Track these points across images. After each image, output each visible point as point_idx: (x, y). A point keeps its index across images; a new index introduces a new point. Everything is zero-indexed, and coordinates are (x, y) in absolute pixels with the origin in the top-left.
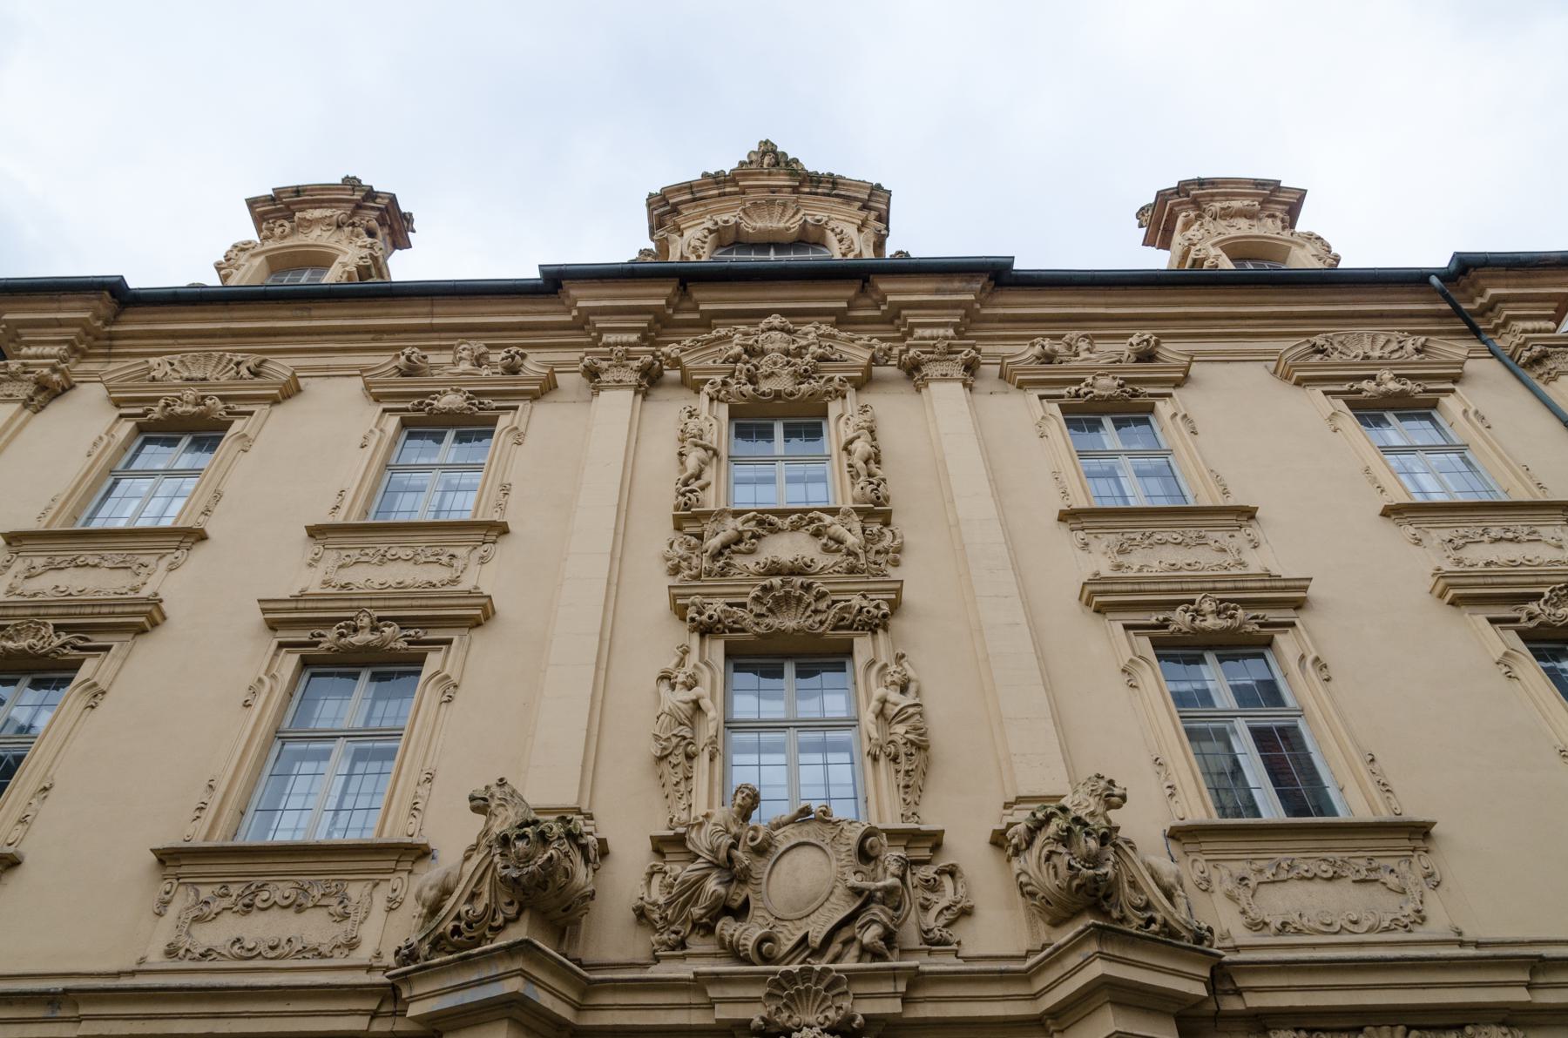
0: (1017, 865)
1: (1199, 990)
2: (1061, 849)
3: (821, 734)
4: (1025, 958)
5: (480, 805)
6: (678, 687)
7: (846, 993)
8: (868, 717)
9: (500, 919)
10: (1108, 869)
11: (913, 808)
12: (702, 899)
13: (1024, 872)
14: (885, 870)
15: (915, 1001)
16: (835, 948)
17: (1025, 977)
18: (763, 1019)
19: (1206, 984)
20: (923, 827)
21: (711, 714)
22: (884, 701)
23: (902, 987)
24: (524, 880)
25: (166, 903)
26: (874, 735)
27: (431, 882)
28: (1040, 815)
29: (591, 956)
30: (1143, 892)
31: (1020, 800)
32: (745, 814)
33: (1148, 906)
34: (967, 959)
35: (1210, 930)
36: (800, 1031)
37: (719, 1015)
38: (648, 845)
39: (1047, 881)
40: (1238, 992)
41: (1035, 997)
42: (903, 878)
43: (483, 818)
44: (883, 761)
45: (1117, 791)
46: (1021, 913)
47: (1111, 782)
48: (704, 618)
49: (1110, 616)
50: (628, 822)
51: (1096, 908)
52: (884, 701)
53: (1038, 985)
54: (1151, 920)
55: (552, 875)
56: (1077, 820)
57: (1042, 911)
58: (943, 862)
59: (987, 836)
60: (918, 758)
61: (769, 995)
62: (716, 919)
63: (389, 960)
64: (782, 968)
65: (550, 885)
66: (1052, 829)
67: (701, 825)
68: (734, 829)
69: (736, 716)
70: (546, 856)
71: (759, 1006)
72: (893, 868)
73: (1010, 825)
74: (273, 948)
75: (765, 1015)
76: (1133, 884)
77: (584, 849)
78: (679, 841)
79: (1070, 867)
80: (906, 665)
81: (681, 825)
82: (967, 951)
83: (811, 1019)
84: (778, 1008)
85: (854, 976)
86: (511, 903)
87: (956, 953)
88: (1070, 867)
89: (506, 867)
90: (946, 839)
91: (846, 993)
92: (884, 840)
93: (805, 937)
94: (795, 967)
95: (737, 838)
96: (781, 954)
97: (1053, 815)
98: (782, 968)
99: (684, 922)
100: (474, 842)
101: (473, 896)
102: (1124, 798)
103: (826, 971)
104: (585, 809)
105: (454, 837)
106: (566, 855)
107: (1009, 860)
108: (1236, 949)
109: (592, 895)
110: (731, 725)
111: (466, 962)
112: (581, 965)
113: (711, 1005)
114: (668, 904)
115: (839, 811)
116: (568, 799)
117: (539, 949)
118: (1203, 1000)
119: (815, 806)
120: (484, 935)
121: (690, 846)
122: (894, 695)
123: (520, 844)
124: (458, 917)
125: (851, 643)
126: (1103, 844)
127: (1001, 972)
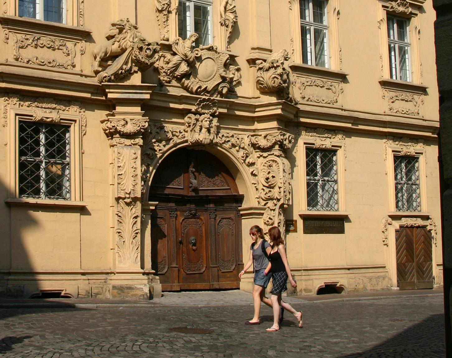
25: (8, 39)
74: (50, 63)
103: (214, 99)
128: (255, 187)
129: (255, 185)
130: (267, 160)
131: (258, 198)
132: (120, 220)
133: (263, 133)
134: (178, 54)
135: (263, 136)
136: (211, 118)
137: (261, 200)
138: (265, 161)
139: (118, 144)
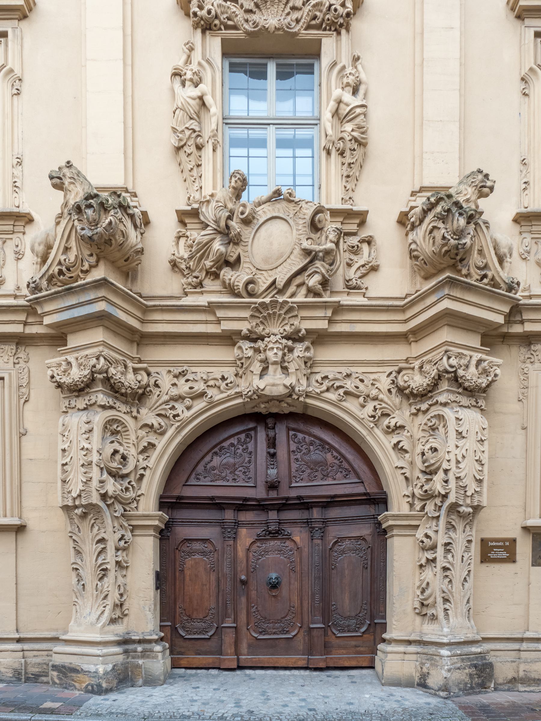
0: (411, 237)
1: (500, 319)
2: (441, 225)
3: (291, 132)
4: (405, 298)
5: (58, 182)
6: (188, 83)
7: (297, 316)
8: (327, 115)
9: (86, 267)
10: (467, 240)
11: (350, 194)
12: (211, 256)
13: (414, 242)
14: (327, 237)
15: (336, 322)
16: (292, 289)
17: (403, 309)
18: (248, 330)
19: (505, 316)
20: (355, 208)
21: (213, 110)
22: (339, 102)
23: (329, 313)
24: (95, 238)
26: (330, 132)
27: (38, 240)
28: (432, 200)
29: (146, 292)
30: (485, 257)
31: (422, 189)
32: (238, 193)
33: (486, 267)
34: (369, 299)
35: (518, 284)
36: (269, 337)
37: (223, 327)
38: (174, 218)
39: (427, 248)
40: (522, 322)
41: (406, 321)
42: (337, 244)
43: (61, 193)
44: (334, 153)
45: (489, 184)
46: (408, 270)
47: (486, 176)
48: (204, 13)
49: (527, 22)
50: (160, 197)
51: (454, 267)
52: (339, 102)
53: (409, 314)
54: (485, 276)
55: (114, 235)
56: (457, 204)
57: (420, 268)
58: (364, 234)
59: (396, 217)
60: (359, 152)
61: (252, 316)
62: (220, 268)
63: (25, 291)
64: (260, 300)
65: (113, 242)
66: (439, 209)
67: (208, 202)
68: (230, 206)
69: (232, 114)
70: (107, 221)
71: (246, 322)
72: (332, 236)
73: (412, 208)
75: (250, 328)
76: (480, 252)
77: (132, 217)
78: (195, 214)
79: (444, 238)
80: (360, 67)
81: (196, 202)
82: (371, 293)
83: (275, 331)
84: (257, 324)
85: (302, 306)
86: (91, 255)
87: (364, 294)
88: (444, 238)
89: (83, 229)
90: (369, 218)
91: (297, 316)
92: (328, 216)
93: (274, 282)
94: (267, 300)
95: (232, 212)
96: (260, 292)
97: (441, 199)
98: (260, 300)
99: (201, 271)
100: (60, 212)
101: (67, 249)
102: (492, 189)
104: (130, 189)
105: (46, 208)
106: (120, 220)
107: (407, 235)
108: (530, 297)
109: (141, 252)
110: (227, 121)
111: (70, 291)
112: (141, 296)
113: (218, 321)
114: (191, 258)
115: (301, 194)
116: (115, 180)
117: (112, 284)
118: (501, 326)
119: (284, 190)
120: (79, 276)
121: (202, 218)
122: (347, 97)
123: (90, 212)
124: (60, 263)
125: (319, 42)
126: (468, 223)
127: (388, 306)
128: (405, 473)
129: (403, 471)
130: (429, 417)
131: (408, 496)
132: (77, 548)
133: (417, 364)
134: (209, 224)
135: (417, 367)
136: (290, 343)
137: (416, 502)
138: (425, 421)
139: (70, 410)
